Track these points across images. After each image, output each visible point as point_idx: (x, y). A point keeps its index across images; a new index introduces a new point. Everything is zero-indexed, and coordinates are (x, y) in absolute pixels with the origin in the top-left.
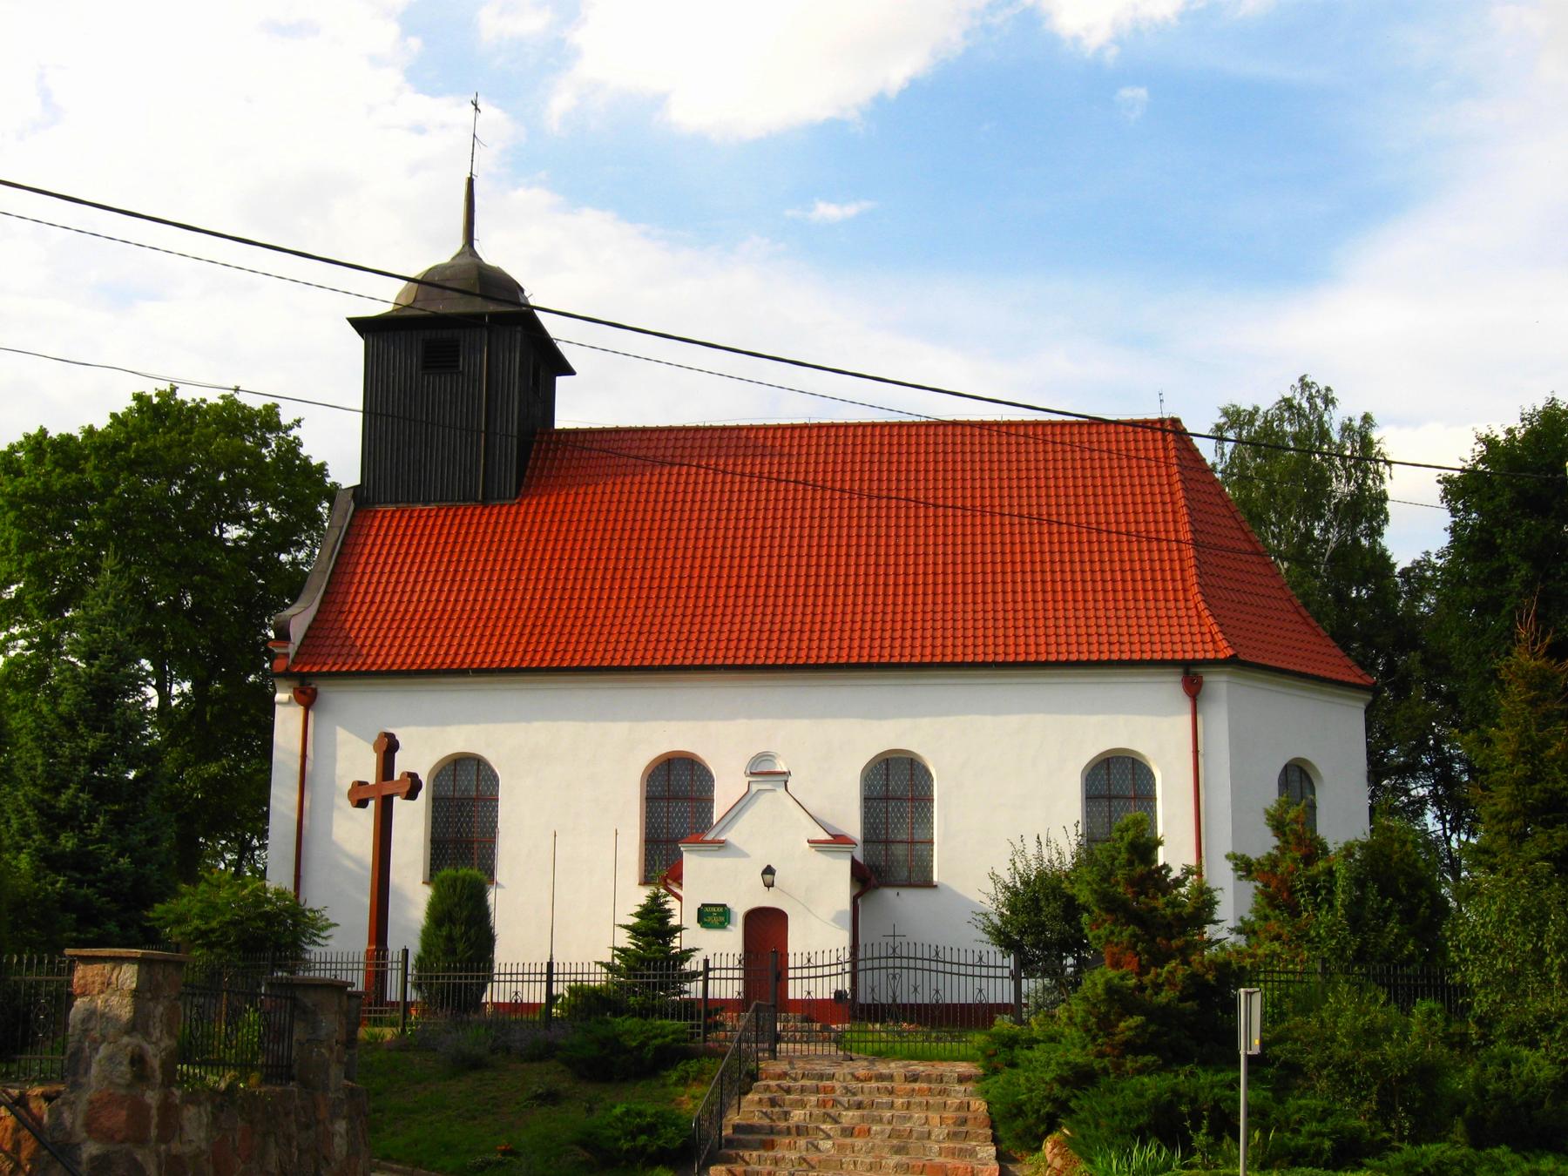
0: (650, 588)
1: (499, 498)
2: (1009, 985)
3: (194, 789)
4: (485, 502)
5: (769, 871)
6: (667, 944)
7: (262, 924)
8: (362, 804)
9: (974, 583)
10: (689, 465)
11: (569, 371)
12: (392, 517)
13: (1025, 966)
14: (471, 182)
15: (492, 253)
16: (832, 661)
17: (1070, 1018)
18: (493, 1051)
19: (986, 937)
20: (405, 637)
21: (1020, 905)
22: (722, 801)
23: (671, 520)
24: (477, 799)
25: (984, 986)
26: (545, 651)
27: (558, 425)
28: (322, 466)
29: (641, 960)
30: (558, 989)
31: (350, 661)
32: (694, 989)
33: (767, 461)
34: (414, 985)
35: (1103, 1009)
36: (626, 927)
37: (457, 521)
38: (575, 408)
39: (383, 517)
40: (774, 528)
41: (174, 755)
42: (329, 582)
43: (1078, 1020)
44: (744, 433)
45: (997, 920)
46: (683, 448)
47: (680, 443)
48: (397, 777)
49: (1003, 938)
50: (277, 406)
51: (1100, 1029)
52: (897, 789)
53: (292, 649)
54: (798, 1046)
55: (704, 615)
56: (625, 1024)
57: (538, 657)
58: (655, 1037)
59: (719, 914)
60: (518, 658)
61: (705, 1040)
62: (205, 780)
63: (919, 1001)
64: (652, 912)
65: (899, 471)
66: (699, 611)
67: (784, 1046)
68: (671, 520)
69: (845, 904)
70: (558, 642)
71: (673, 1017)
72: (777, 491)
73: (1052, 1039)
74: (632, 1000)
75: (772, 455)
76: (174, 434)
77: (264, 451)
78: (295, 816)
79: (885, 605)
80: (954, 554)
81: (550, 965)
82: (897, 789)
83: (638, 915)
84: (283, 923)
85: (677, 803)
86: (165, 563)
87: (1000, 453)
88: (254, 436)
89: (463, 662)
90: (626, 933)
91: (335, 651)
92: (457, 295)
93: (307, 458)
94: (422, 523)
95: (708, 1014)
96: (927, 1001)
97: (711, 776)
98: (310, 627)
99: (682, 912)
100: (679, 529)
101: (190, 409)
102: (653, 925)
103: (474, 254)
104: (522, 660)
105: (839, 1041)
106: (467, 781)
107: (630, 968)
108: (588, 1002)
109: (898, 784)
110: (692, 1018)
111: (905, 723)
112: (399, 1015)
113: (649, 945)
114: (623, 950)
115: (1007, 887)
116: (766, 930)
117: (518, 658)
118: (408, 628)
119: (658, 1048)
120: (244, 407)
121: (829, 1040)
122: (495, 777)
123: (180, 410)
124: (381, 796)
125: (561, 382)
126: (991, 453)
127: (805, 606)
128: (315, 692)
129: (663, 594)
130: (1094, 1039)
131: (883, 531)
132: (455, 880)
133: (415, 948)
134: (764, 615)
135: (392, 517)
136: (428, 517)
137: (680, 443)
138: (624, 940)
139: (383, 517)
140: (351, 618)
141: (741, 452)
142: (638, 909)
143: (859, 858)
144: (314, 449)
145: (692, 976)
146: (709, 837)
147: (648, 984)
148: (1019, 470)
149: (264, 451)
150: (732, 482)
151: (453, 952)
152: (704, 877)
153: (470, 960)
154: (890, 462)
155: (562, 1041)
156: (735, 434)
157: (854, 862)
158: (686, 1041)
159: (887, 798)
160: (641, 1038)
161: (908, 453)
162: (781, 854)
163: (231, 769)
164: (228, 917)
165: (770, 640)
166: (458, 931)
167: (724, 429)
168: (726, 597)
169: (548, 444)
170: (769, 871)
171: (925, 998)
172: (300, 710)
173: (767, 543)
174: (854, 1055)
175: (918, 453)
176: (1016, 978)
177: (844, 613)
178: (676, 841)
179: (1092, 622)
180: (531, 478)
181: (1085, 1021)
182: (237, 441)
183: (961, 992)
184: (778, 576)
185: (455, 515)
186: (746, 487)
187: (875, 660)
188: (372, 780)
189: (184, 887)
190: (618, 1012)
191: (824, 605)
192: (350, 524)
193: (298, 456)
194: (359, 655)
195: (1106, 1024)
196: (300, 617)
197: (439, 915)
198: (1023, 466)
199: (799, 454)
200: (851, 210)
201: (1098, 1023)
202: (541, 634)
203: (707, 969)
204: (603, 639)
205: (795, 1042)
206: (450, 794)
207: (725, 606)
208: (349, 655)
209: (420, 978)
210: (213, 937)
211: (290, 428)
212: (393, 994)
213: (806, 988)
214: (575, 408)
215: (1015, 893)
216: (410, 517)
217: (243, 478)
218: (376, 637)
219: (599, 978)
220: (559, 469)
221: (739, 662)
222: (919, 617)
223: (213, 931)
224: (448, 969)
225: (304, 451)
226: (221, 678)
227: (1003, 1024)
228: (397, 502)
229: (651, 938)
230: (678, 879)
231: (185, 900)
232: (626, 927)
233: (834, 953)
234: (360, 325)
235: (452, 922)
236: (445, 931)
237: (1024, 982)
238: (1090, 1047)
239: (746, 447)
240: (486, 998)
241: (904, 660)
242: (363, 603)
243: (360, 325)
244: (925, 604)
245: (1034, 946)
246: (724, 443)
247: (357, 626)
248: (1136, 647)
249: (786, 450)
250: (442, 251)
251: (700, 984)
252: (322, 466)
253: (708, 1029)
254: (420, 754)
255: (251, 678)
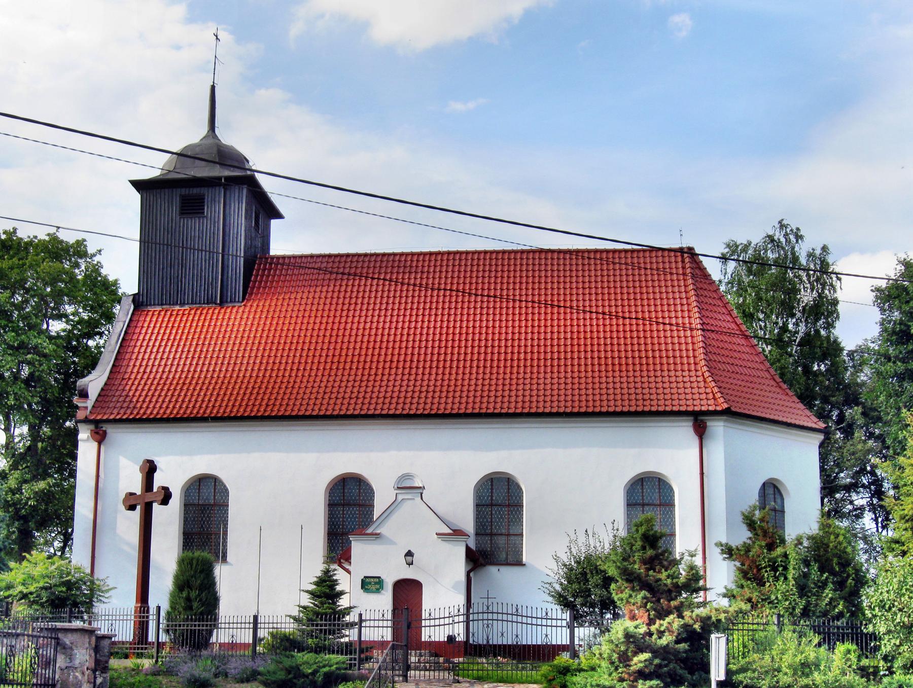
0: (332, 362)
1: (231, 301)
2: (566, 632)
3: (29, 499)
4: (222, 303)
5: (409, 554)
6: (334, 603)
7: (64, 589)
8: (132, 508)
9: (545, 359)
10: (379, 279)
11: (279, 216)
12: (159, 314)
13: (577, 618)
14: (213, 88)
15: (228, 137)
16: (454, 412)
17: (601, 654)
18: (216, 675)
19: (551, 599)
20: (166, 396)
21: (573, 577)
22: (379, 505)
23: (347, 316)
24: (214, 505)
25: (549, 633)
26: (260, 405)
27: (272, 252)
28: (116, 283)
29: (317, 614)
30: (261, 633)
31: (129, 412)
32: (350, 635)
33: (413, 276)
34: (164, 630)
35: (623, 648)
36: (307, 591)
37: (203, 318)
38: (284, 242)
39: (153, 315)
40: (416, 322)
41: (16, 476)
42: (116, 359)
43: (605, 656)
44: (397, 258)
45: (558, 588)
46: (356, 267)
47: (354, 265)
48: (155, 490)
49: (564, 602)
50: (85, 240)
51: (620, 662)
52: (499, 500)
53: (90, 403)
54: (427, 673)
55: (368, 381)
56: (301, 657)
57: (255, 409)
58: (324, 666)
59: (376, 583)
60: (242, 410)
61: (359, 669)
62: (37, 492)
63: (505, 643)
64: (325, 581)
65: (502, 283)
66: (365, 378)
67: (413, 672)
68: (347, 316)
69: (462, 578)
70: (269, 399)
71: (338, 653)
72: (432, 296)
73: (593, 669)
74: (310, 641)
75: (416, 272)
76: (15, 260)
77: (77, 271)
78: (91, 516)
79: (491, 374)
80: (539, 339)
81: (256, 618)
82: (499, 500)
83: (316, 584)
84: (79, 588)
85: (349, 509)
86: (11, 347)
87: (571, 271)
88: (70, 261)
89: (204, 413)
90: (307, 596)
91: (119, 405)
92: (203, 163)
93: (106, 276)
94: (178, 319)
95: (362, 651)
96: (510, 643)
97: (372, 490)
98: (102, 389)
99: (345, 581)
100: (359, 323)
101: (26, 243)
102: (326, 591)
103: (215, 137)
104: (245, 411)
105: (454, 669)
106: (207, 495)
107: (309, 620)
108: (285, 644)
109: (500, 495)
110: (351, 654)
111: (504, 454)
112: (154, 650)
113: (322, 603)
114: (304, 608)
115: (565, 565)
116: (407, 594)
117: (242, 410)
118: (169, 390)
119: (326, 674)
120: (62, 241)
121: (448, 669)
122: (227, 490)
123: (19, 243)
124: (146, 501)
125: (274, 223)
126: (559, 271)
127: (437, 374)
128: (105, 433)
129: (341, 366)
130: (616, 669)
131: (491, 324)
132: (192, 559)
133: (165, 606)
134: (409, 380)
135: (159, 314)
136: (183, 314)
137: (354, 265)
138: (306, 600)
139: (153, 315)
140: (130, 383)
141: (395, 270)
142: (315, 579)
143: (472, 546)
144: (110, 271)
145: (351, 625)
146: (369, 531)
147: (321, 630)
148: (584, 282)
149: (77, 271)
150: (407, 290)
151: (191, 608)
152: (366, 556)
153: (202, 613)
154: (496, 277)
155: (261, 669)
156: (391, 258)
157: (468, 549)
158: (346, 669)
159: (492, 505)
160: (315, 667)
161: (509, 271)
162: (418, 543)
163: (55, 485)
164: (41, 584)
165: (412, 398)
166: (193, 594)
167: (384, 255)
168: (384, 368)
169: (265, 265)
170: (409, 554)
171: (508, 640)
172: (96, 444)
173: (412, 332)
174: (461, 679)
175: (515, 271)
176: (571, 628)
177: (463, 380)
178: (347, 534)
179: (597, 386)
180: (253, 288)
181: (610, 657)
182: (57, 265)
183: (533, 637)
184: (419, 354)
185: (201, 314)
186: (410, 294)
187: (484, 411)
188: (139, 492)
189: (12, 564)
190: (301, 649)
191: (450, 374)
192: (131, 320)
193: (100, 275)
194: (134, 407)
195: (624, 659)
196: (94, 383)
197: (182, 584)
198: (587, 279)
199: (434, 272)
200: (471, 105)
201: (619, 658)
202: (258, 393)
203: (361, 621)
204: (299, 397)
205: (426, 670)
206: (196, 502)
207: (383, 375)
208: (128, 407)
209: (168, 626)
210: (32, 598)
211: (94, 255)
212: (152, 637)
213: (380, 634)
214: (284, 242)
215: (571, 570)
216: (171, 315)
217: (61, 290)
218: (186, 395)
219: (289, 628)
220: (272, 282)
221: (391, 412)
222: (514, 382)
223: (31, 593)
224: (187, 620)
225: (104, 272)
226: (49, 423)
227: (564, 658)
228: (162, 304)
229: (324, 599)
230: (348, 559)
231: (13, 572)
232: (307, 591)
233: (447, 610)
234: (139, 185)
235: (190, 587)
236: (184, 594)
237: (576, 629)
238: (614, 674)
239: (399, 267)
240: (213, 639)
241: (503, 411)
242: (138, 372)
243: (139, 185)
244: (518, 373)
245: (582, 605)
246: (384, 264)
247: (134, 388)
248: (633, 403)
249: (426, 269)
250: (191, 134)
251: (356, 630)
252: (116, 283)
253: (361, 661)
254: (174, 474)
255: (68, 424)
